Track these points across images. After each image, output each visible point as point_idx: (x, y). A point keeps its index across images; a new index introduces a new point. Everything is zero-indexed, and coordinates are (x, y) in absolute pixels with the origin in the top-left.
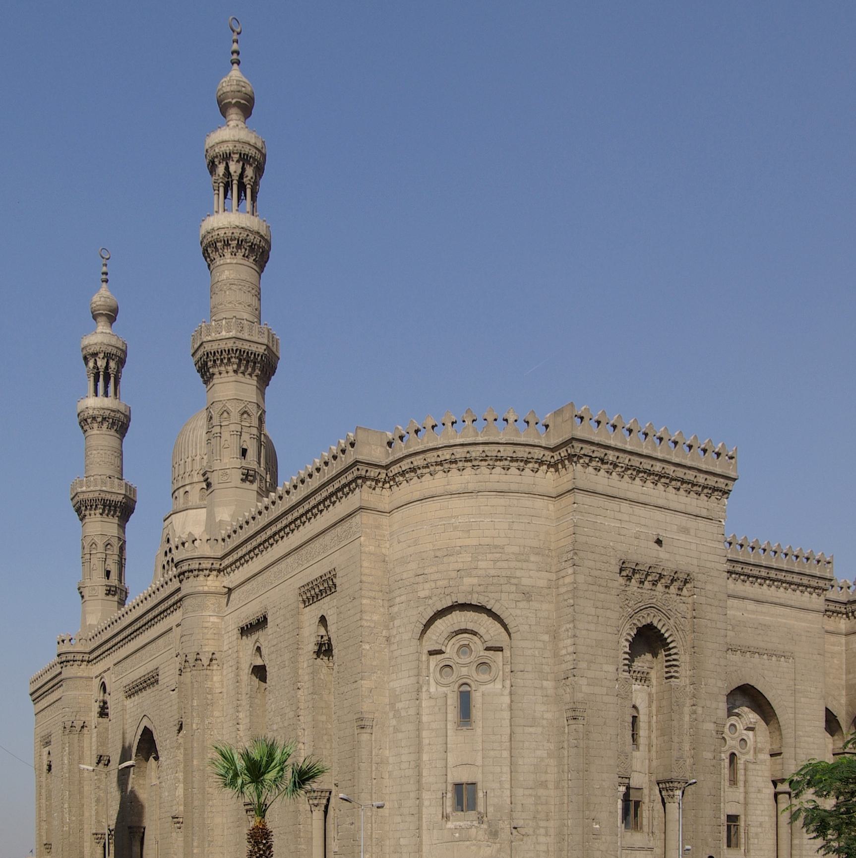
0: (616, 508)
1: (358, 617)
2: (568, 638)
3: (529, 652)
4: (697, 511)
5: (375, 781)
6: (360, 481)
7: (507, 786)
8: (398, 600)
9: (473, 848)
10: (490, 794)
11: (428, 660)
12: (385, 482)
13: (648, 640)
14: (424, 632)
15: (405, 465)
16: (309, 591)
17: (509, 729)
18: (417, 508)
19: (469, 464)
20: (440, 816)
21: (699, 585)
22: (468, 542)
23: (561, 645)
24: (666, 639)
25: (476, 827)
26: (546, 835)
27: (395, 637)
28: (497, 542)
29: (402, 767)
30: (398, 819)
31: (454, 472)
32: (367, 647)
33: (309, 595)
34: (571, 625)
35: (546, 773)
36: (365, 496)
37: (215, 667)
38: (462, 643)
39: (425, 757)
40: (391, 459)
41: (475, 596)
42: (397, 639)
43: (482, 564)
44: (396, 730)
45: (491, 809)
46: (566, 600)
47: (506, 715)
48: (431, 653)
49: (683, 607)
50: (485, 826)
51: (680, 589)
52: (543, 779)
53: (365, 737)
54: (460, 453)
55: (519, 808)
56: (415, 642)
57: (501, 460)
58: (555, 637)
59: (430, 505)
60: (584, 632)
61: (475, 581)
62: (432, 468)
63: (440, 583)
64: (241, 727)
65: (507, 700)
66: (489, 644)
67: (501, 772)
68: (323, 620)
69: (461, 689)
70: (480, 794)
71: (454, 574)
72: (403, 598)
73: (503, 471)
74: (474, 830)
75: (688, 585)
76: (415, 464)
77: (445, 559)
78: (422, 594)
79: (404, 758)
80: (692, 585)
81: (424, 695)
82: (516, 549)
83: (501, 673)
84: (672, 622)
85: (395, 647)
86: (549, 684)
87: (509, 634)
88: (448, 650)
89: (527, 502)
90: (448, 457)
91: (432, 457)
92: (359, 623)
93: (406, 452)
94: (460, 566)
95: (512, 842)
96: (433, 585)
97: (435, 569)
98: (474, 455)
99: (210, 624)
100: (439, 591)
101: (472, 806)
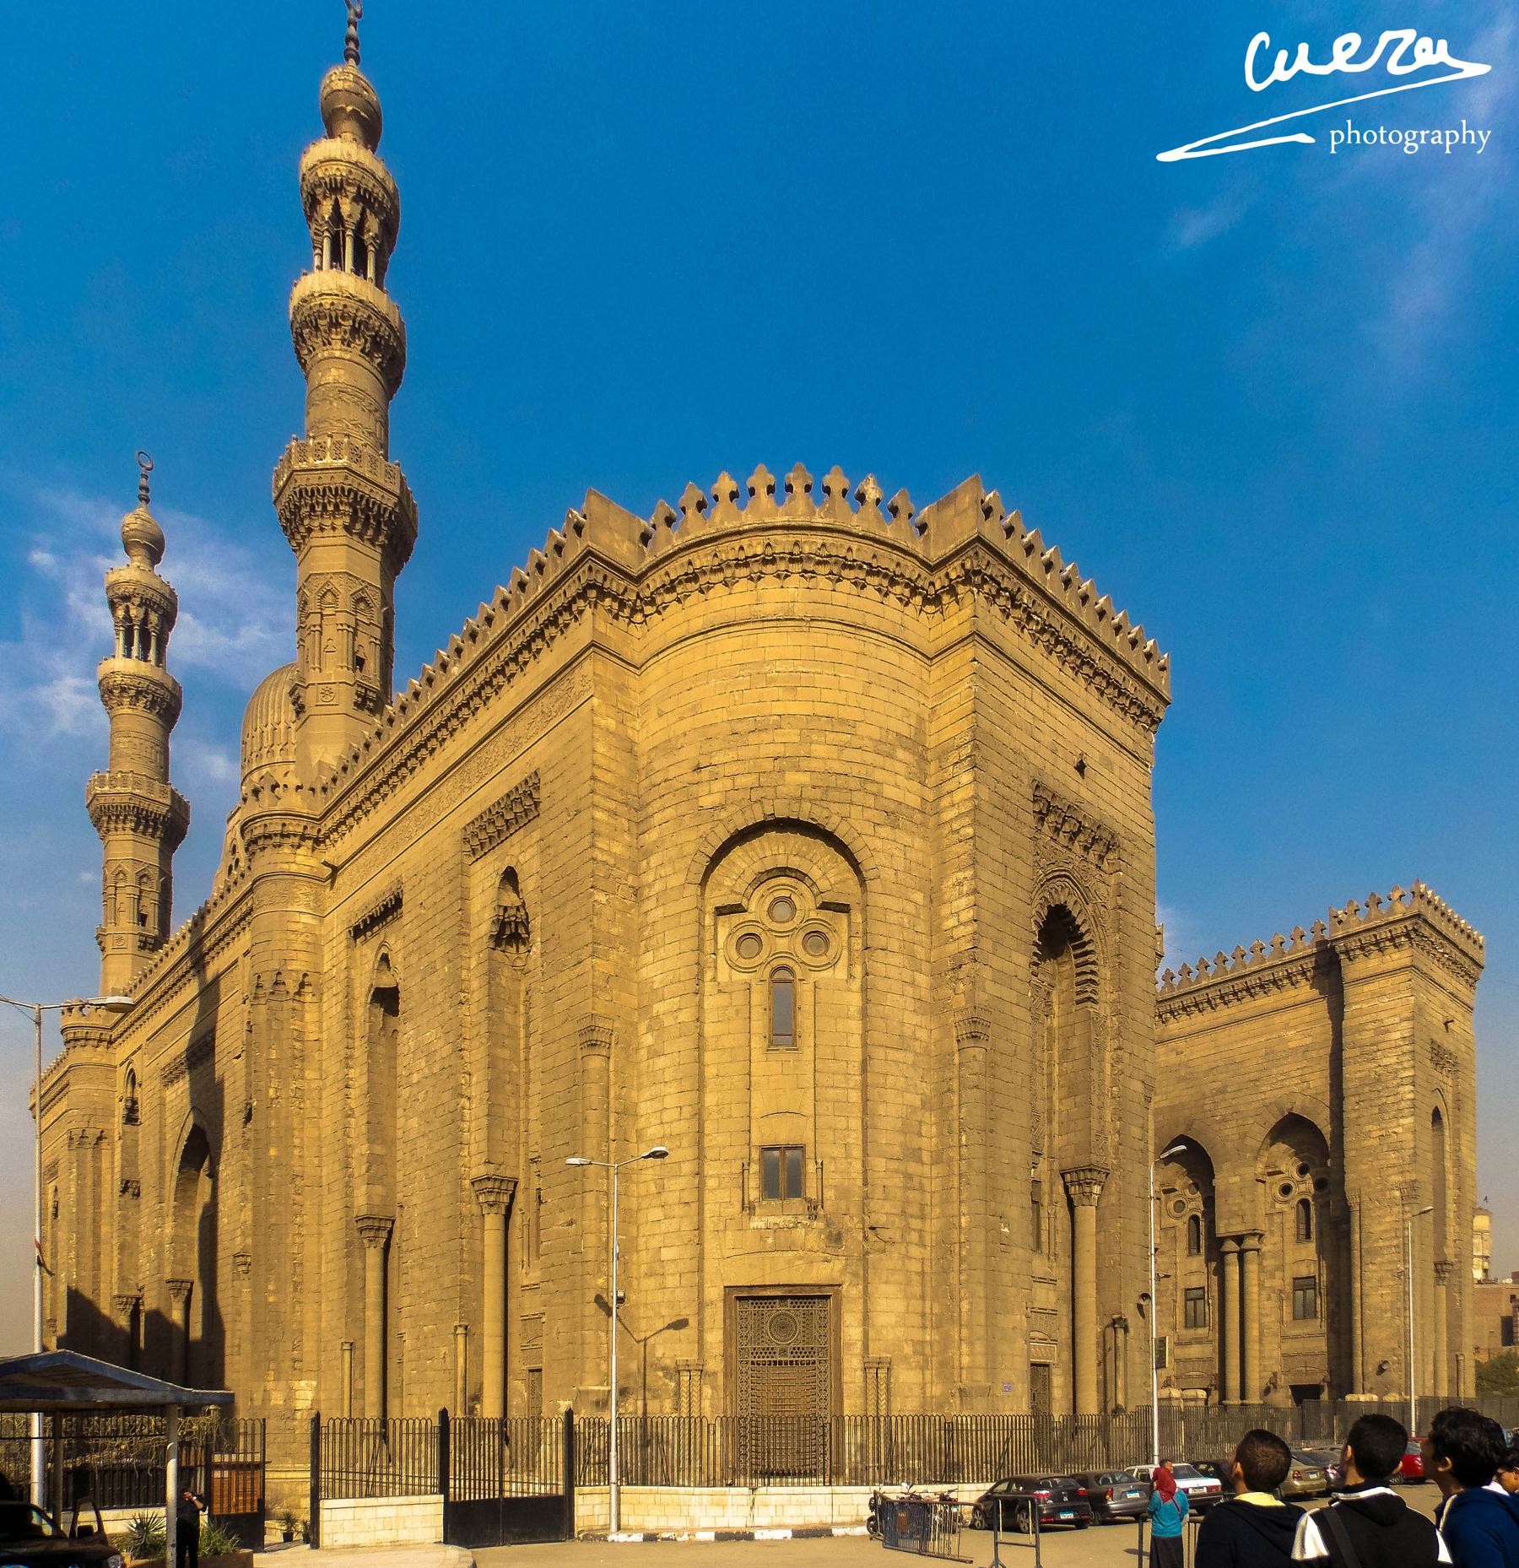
0: (1028, 691)
1: (586, 843)
2: (961, 895)
3: (893, 918)
4: (1122, 739)
5: (613, 1145)
6: (593, 594)
7: (857, 1152)
8: (657, 818)
10: (829, 1167)
11: (715, 924)
12: (634, 611)
13: (1058, 933)
14: (709, 870)
15: (676, 569)
16: (482, 828)
17: (859, 1051)
18: (698, 648)
19: (797, 568)
20: (739, 1206)
21: (1125, 856)
22: (794, 708)
23: (945, 910)
24: (1082, 935)
25: (805, 1226)
26: (922, 1244)
27: (650, 886)
28: (845, 713)
30: (657, 1213)
31: (769, 582)
32: (602, 898)
33: (483, 836)
34: (969, 873)
35: (920, 1135)
36: (602, 627)
37: (308, 998)
38: (777, 894)
39: (710, 1099)
40: (649, 560)
41: (806, 806)
42: (658, 887)
43: (819, 750)
44: (654, 1053)
45: (829, 1194)
46: (957, 831)
47: (855, 1026)
48: (721, 911)
49: (1102, 889)
50: (819, 1224)
51: (1101, 858)
52: (915, 1145)
53: (595, 1063)
54: (782, 543)
55: (879, 1193)
56: (693, 890)
57: (851, 567)
58: (934, 898)
59: (726, 643)
60: (988, 887)
61: (805, 778)
62: (728, 573)
63: (742, 781)
64: (353, 1093)
65: (855, 1000)
66: (828, 898)
67: (847, 1129)
68: (510, 877)
69: (776, 977)
70: (811, 1167)
71: (768, 765)
72: (670, 813)
73: (855, 590)
74: (801, 1231)
75: (1111, 856)
76: (697, 564)
77: (752, 738)
78: (706, 802)
79: (670, 1102)
80: (1116, 855)
81: (709, 987)
82: (876, 733)
83: (845, 952)
84: (1090, 908)
85: (651, 904)
86: (923, 980)
87: (863, 882)
88: (752, 908)
89: (890, 653)
90: (759, 550)
91: (728, 550)
92: (588, 854)
93: (678, 543)
94: (779, 750)
95: (867, 1253)
96: (728, 784)
97: (732, 755)
98: (807, 549)
99: (300, 926)
100: (741, 794)
101: (795, 1188)
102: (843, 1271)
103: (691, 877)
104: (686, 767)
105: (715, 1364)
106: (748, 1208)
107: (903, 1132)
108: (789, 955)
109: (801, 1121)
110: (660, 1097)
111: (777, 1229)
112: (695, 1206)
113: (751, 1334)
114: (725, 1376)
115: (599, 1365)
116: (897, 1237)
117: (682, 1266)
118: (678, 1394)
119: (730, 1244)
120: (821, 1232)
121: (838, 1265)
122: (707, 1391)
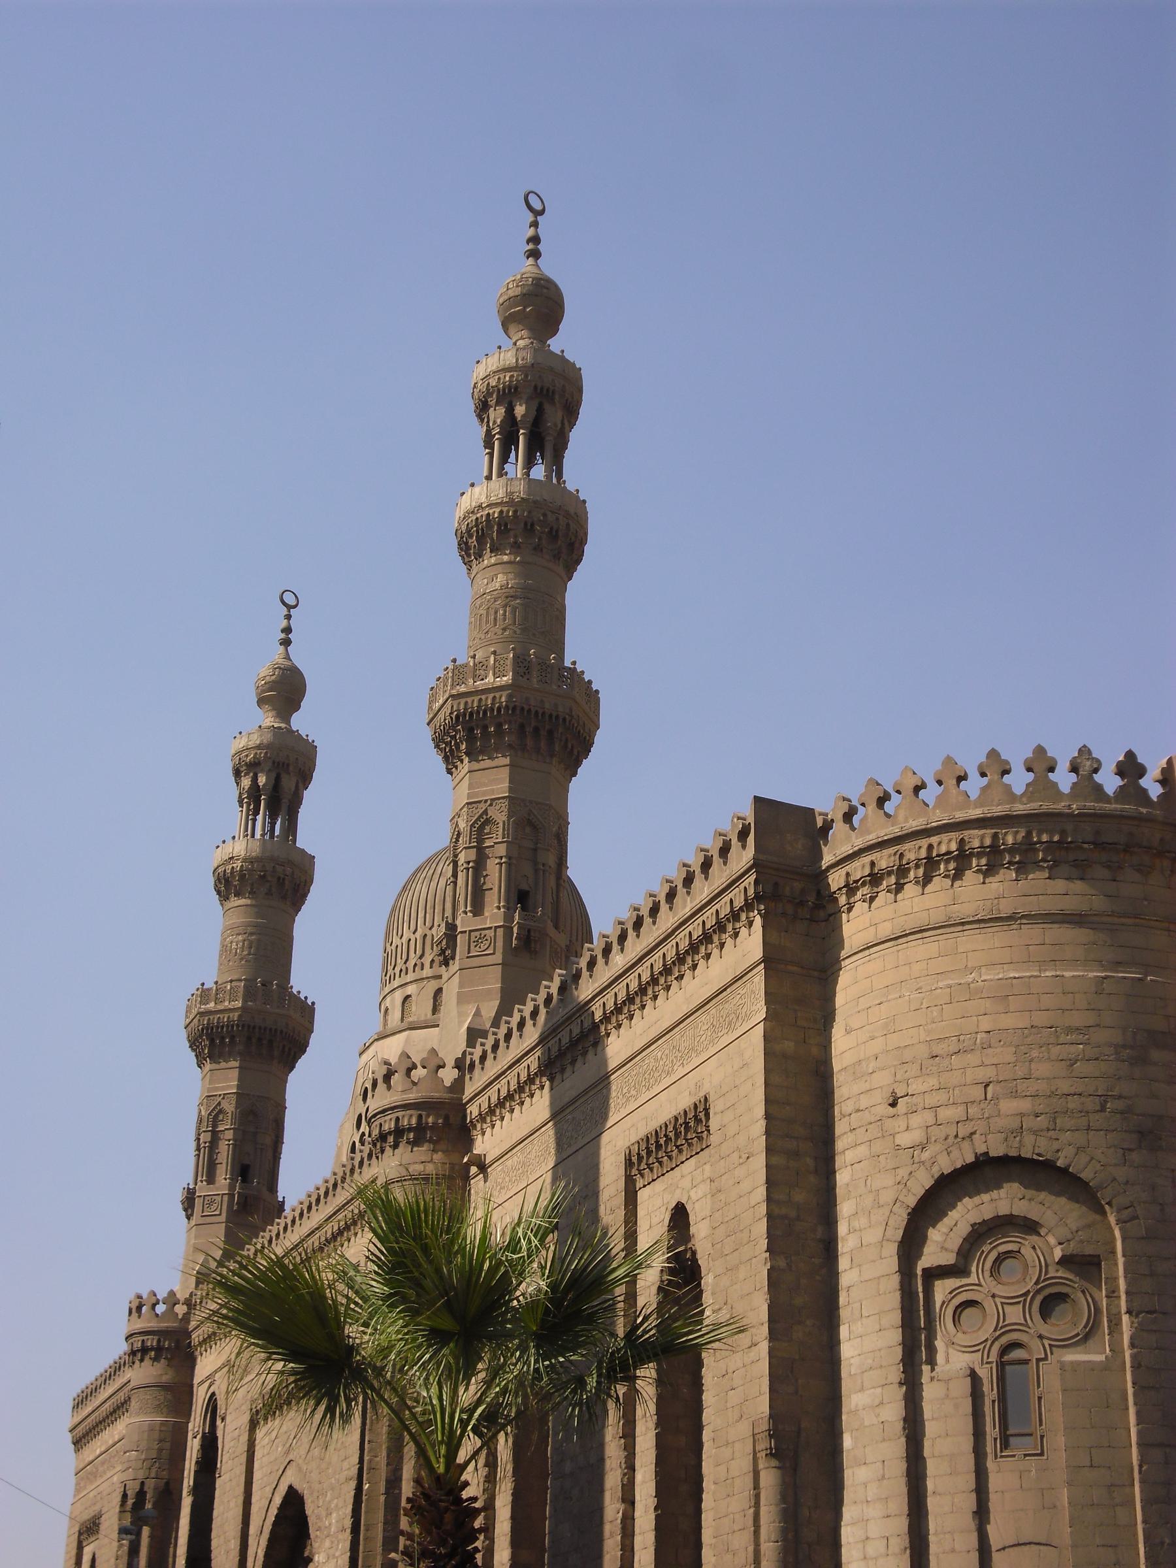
29: (871, 1551)
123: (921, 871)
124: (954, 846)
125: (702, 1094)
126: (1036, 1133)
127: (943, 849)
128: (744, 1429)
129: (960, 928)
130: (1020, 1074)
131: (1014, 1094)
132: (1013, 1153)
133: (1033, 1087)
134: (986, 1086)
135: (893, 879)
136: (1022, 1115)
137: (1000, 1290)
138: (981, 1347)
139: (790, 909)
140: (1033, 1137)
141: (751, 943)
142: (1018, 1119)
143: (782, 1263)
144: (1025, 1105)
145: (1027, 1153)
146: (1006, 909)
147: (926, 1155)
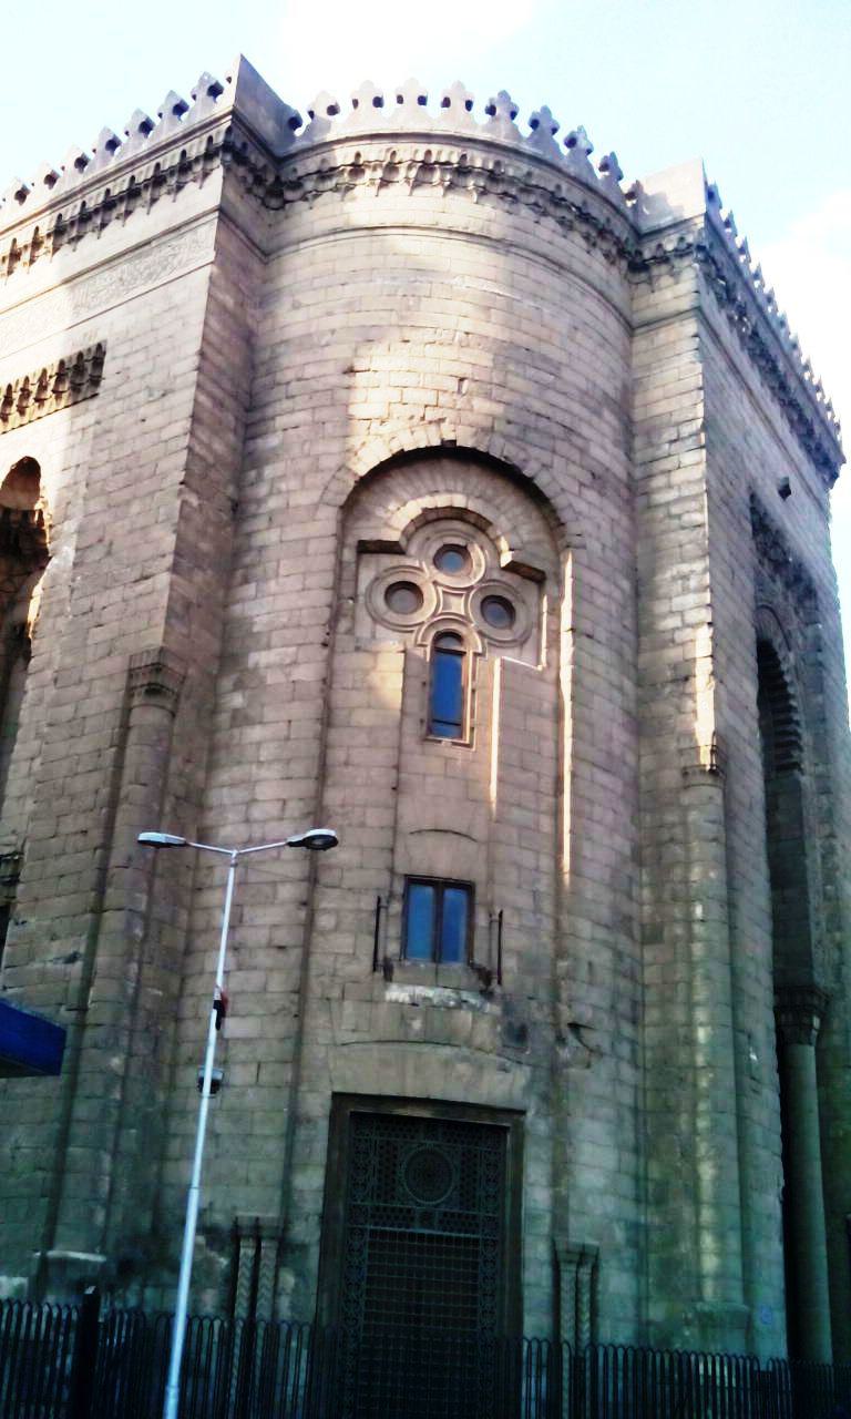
9: (462, 1068)
20: (367, 962)
25: (472, 1008)
29: (256, 813)
45: (510, 963)
50: (493, 1009)
74: (465, 1017)
102: (528, 1089)
103: (329, 496)
104: (330, 368)
105: (306, 1231)
106: (384, 969)
107: (612, 888)
108: (463, 620)
109: (470, 847)
110: (250, 783)
111: (430, 1007)
112: (295, 955)
113: (374, 1181)
114: (323, 1254)
115: (92, 1213)
116: (606, 1046)
117: (261, 1051)
118: (231, 1279)
119: (348, 1023)
120: (496, 1021)
121: (521, 1077)
122: (288, 1279)
123: (413, 173)
124: (455, 159)
125: (93, 343)
126: (507, 437)
127: (443, 159)
128: (117, 663)
129: (446, 235)
130: (495, 381)
131: (488, 396)
132: (482, 448)
133: (507, 397)
134: (462, 380)
135: (379, 173)
136: (494, 418)
137: (442, 578)
138: (416, 629)
139: (250, 179)
140: (502, 441)
141: (207, 192)
142: (490, 419)
143: (194, 500)
144: (498, 409)
145: (496, 453)
146: (496, 231)
147: (386, 429)
